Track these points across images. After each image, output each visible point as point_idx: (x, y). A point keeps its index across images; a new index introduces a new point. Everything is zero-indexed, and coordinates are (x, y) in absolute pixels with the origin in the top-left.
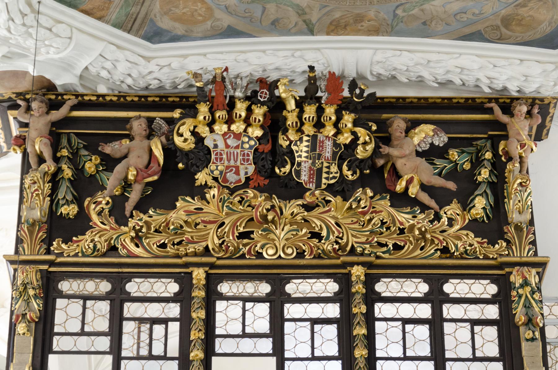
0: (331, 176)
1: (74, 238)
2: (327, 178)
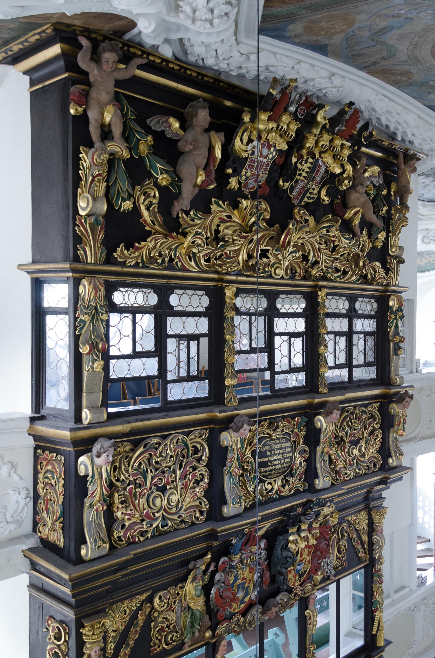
0: (312, 196)
1: (137, 244)
2: (308, 198)
